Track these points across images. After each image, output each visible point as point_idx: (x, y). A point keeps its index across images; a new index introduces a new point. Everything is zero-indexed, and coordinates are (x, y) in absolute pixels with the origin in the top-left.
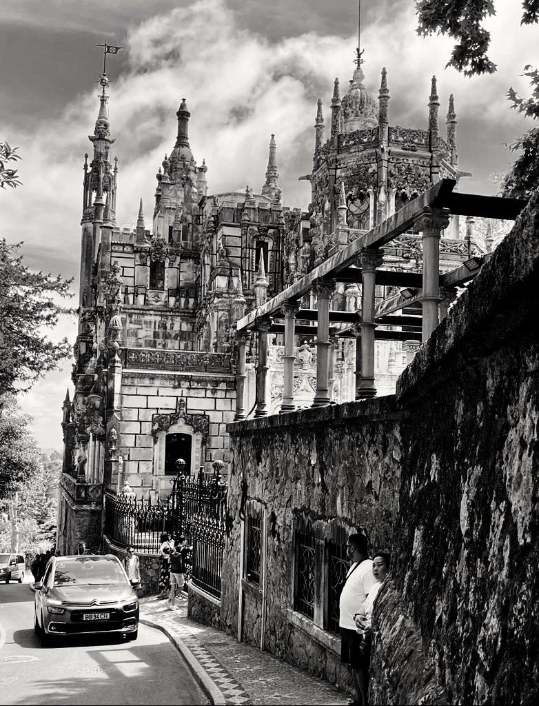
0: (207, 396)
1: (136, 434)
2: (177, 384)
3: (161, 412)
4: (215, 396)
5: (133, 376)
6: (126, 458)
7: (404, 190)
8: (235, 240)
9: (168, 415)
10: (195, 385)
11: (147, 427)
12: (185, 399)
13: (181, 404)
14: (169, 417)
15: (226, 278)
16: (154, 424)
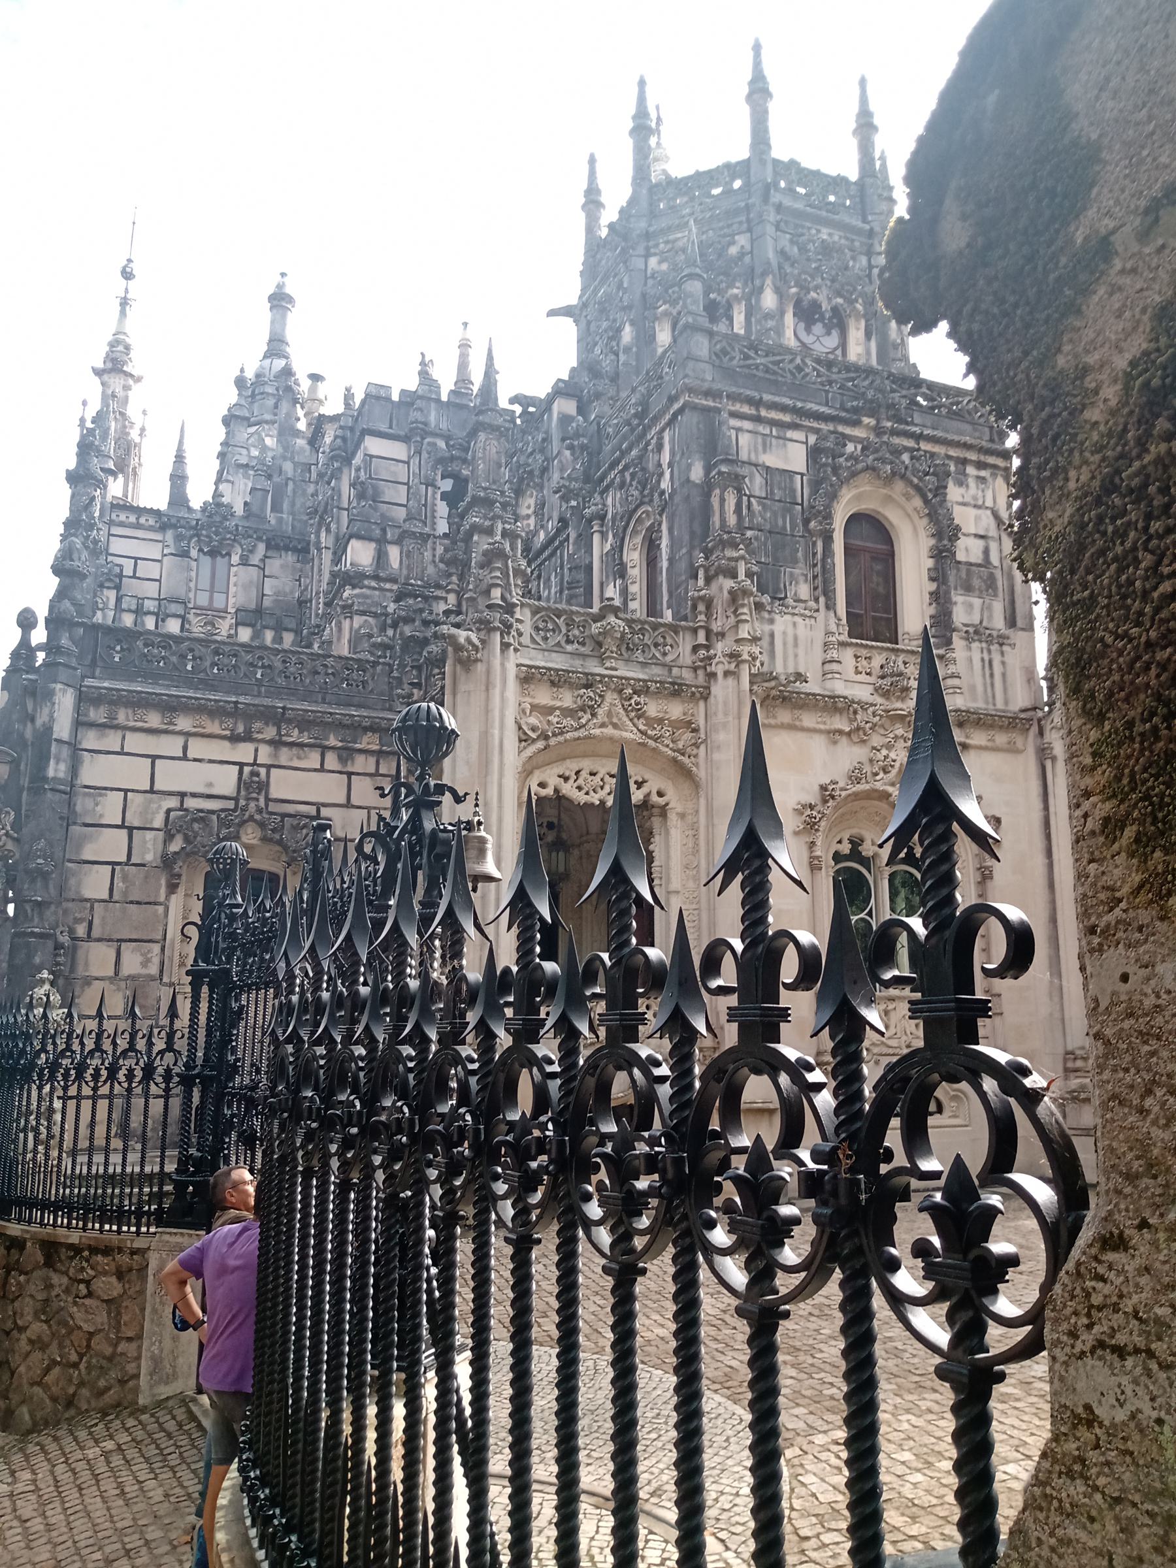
0: (326, 767)
1: (114, 864)
2: (240, 729)
3: (191, 803)
4: (350, 769)
5: (115, 700)
6: (81, 931)
7: (813, 294)
8: (393, 468)
9: (212, 812)
10: (295, 736)
11: (150, 845)
12: (263, 771)
13: (253, 783)
14: (214, 817)
15: (373, 545)
16: (169, 837)
